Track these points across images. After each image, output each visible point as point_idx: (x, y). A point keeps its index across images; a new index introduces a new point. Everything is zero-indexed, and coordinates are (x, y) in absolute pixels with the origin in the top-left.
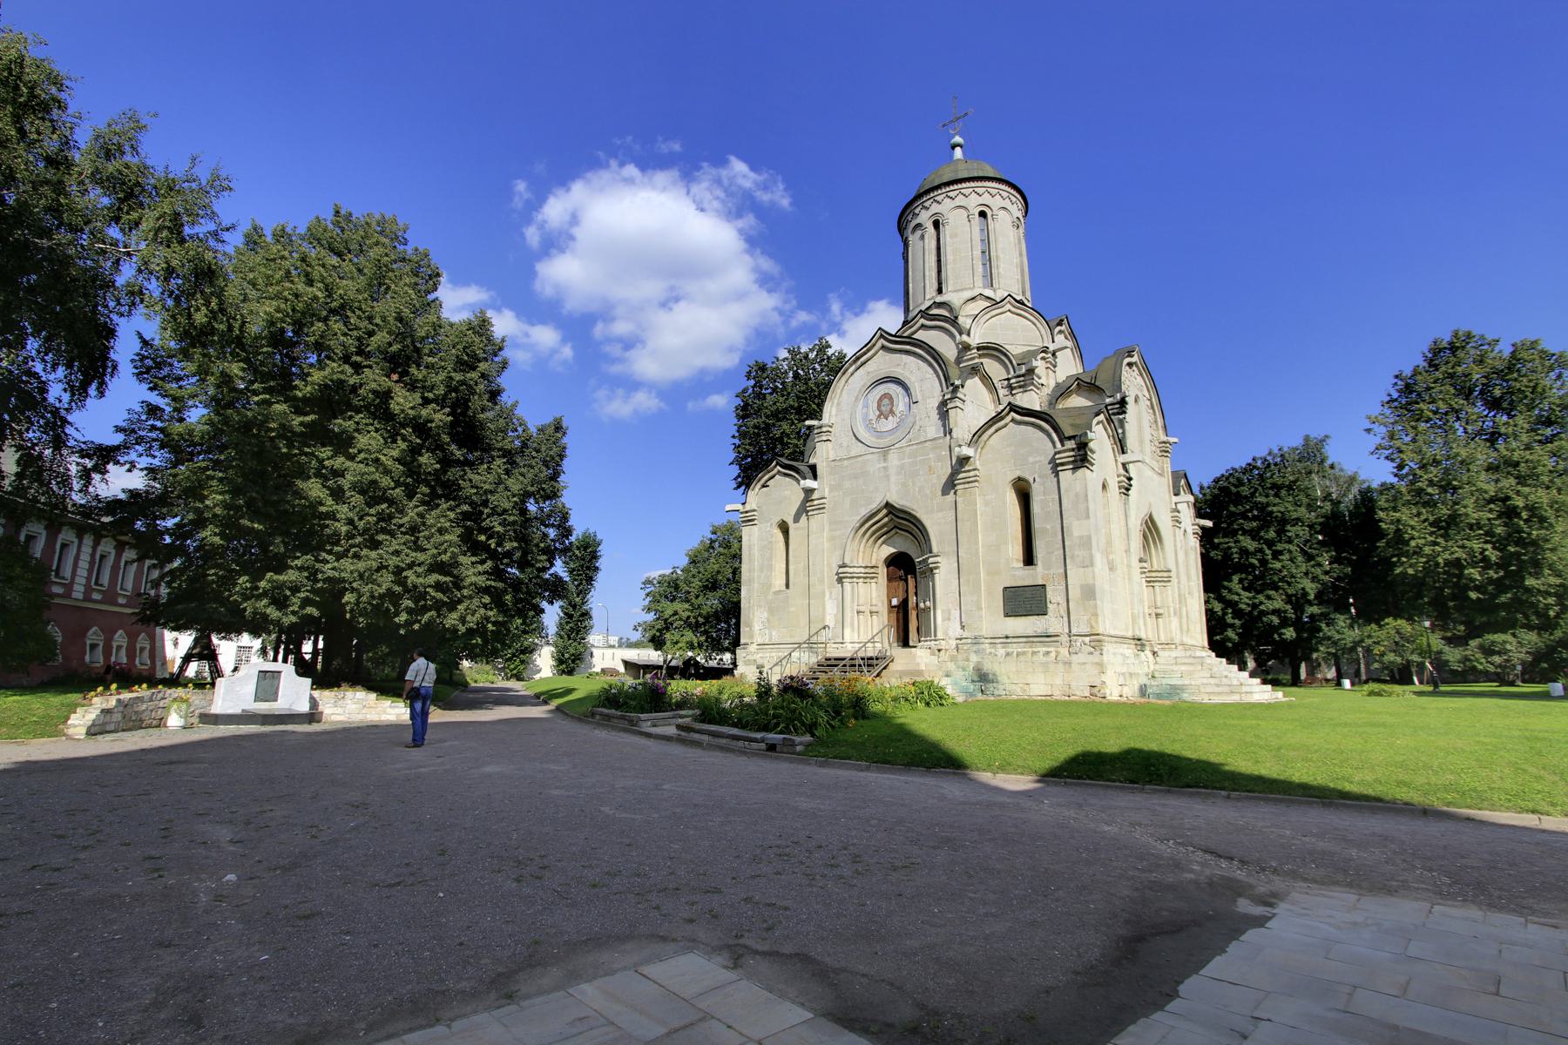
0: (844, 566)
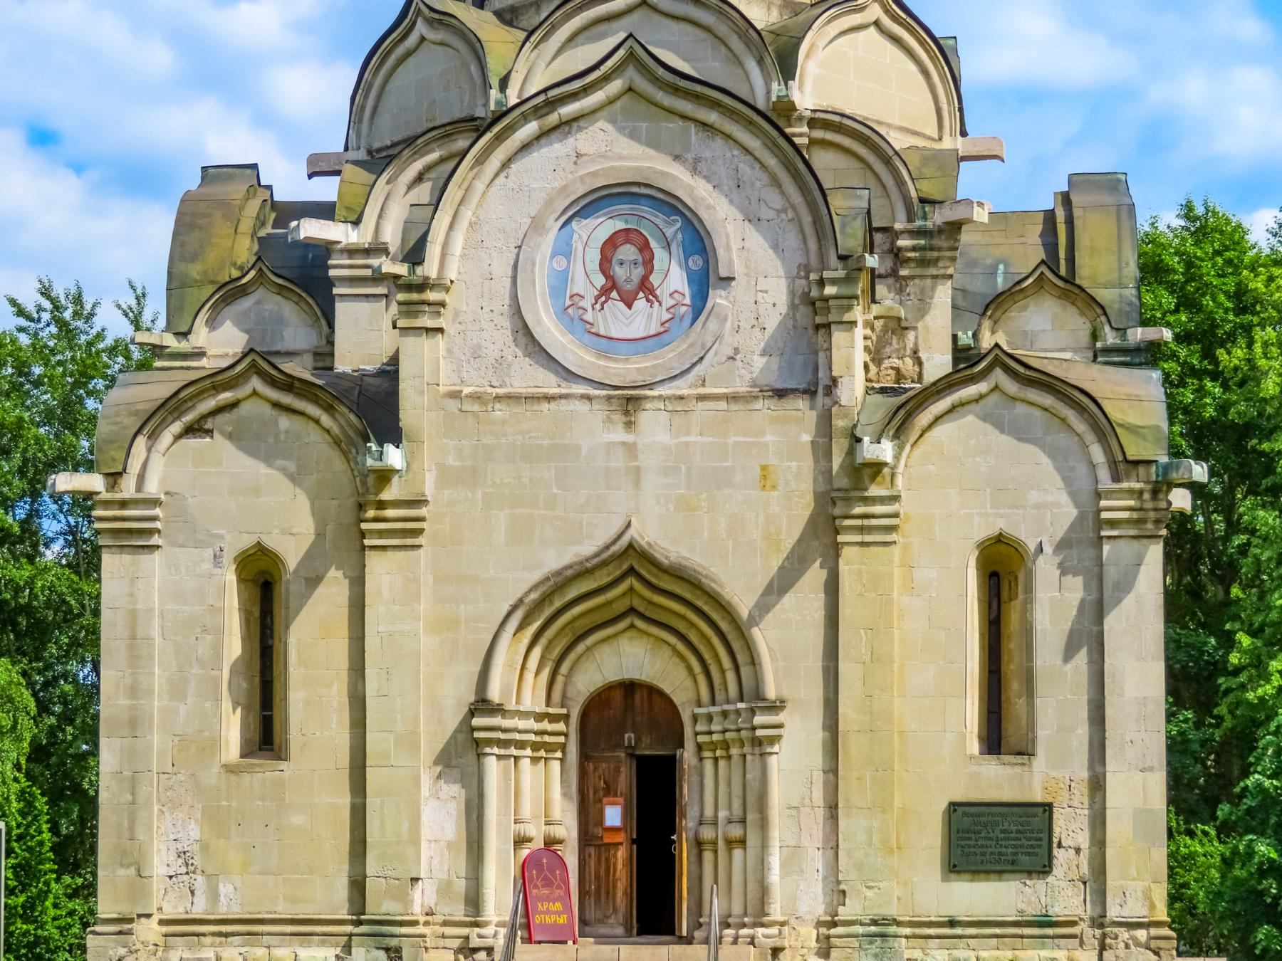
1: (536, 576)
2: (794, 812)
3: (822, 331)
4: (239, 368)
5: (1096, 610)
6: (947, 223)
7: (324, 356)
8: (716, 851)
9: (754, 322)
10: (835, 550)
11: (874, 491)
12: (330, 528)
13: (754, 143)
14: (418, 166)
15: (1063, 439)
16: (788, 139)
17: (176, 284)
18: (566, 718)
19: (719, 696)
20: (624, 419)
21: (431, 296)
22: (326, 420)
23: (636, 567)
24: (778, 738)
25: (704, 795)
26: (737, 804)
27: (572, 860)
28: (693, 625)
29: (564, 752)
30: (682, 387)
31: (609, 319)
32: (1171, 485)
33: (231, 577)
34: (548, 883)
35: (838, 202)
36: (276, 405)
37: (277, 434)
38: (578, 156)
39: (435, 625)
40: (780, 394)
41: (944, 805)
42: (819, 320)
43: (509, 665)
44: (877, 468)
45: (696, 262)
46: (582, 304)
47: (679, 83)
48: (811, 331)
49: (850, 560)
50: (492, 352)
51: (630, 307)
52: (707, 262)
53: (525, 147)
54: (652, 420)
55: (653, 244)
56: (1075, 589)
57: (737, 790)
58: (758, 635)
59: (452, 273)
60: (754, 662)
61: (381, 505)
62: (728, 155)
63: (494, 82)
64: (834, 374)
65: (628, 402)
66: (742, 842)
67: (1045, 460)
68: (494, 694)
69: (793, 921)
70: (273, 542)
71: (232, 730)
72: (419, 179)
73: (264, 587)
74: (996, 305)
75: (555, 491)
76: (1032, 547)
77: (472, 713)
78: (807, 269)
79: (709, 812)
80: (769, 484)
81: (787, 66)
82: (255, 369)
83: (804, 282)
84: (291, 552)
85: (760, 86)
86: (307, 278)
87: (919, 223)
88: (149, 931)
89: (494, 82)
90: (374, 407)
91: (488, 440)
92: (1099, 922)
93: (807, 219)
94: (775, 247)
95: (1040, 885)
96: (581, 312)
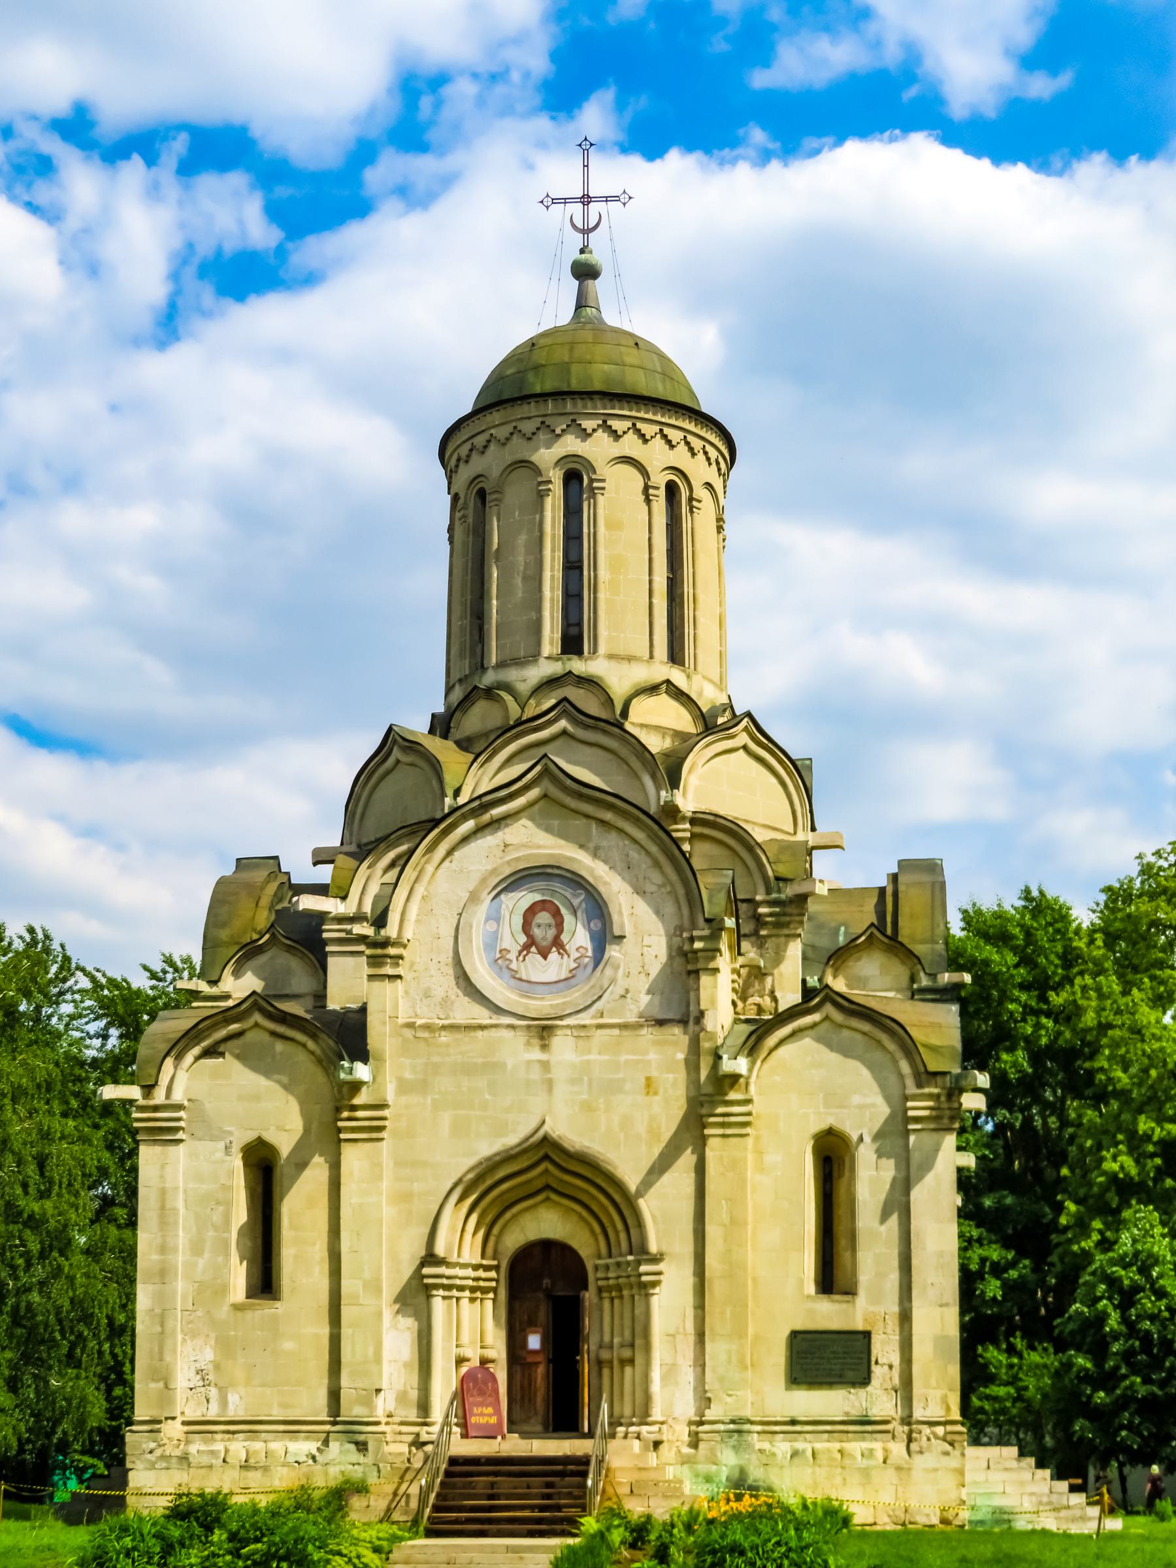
1: (472, 1161)
2: (670, 1338)
3: (693, 976)
5: (904, 1185)
7: (320, 997)
8: (612, 1368)
9: (640, 969)
10: (701, 1144)
11: (733, 1096)
13: (640, 835)
14: (391, 855)
15: (878, 1055)
16: (668, 834)
17: (210, 944)
18: (497, 1268)
20: (540, 1042)
21: (392, 951)
23: (550, 1154)
24: (655, 1284)
25: (600, 1325)
26: (627, 1333)
27: (502, 1376)
28: (593, 1197)
29: (495, 1294)
30: (585, 1019)
32: (961, 1091)
33: (238, 1163)
34: (482, 1393)
35: (706, 882)
38: (506, 846)
39: (396, 1196)
40: (661, 1023)
42: (690, 967)
43: (452, 1228)
44: (734, 1079)
45: (596, 925)
46: (508, 956)
47: (583, 791)
48: (684, 976)
49: (715, 1149)
50: (439, 993)
51: (545, 958)
52: (604, 925)
53: (465, 839)
54: (563, 1045)
55: (563, 911)
56: (888, 1170)
57: (627, 1322)
58: (642, 1203)
59: (408, 934)
60: (640, 1224)
61: (354, 1108)
62: (621, 844)
63: (450, 792)
64: (702, 1007)
65: (543, 1031)
66: (631, 1361)
67: (865, 1073)
68: (440, 1250)
69: (670, 1421)
70: (271, 1137)
71: (238, 1276)
72: (392, 865)
73: (265, 1172)
74: (838, 957)
75: (487, 1097)
76: (855, 1138)
77: (423, 1264)
78: (680, 929)
79: (607, 1338)
80: (651, 1090)
81: (674, 781)
82: (256, 1007)
83: (678, 939)
84: (284, 1145)
85: (655, 796)
86: (307, 940)
87: (774, 895)
88: (173, 1430)
89: (450, 792)
90: (349, 1035)
91: (436, 1059)
92: (907, 1420)
93: (681, 891)
94: (657, 912)
95: (861, 1392)
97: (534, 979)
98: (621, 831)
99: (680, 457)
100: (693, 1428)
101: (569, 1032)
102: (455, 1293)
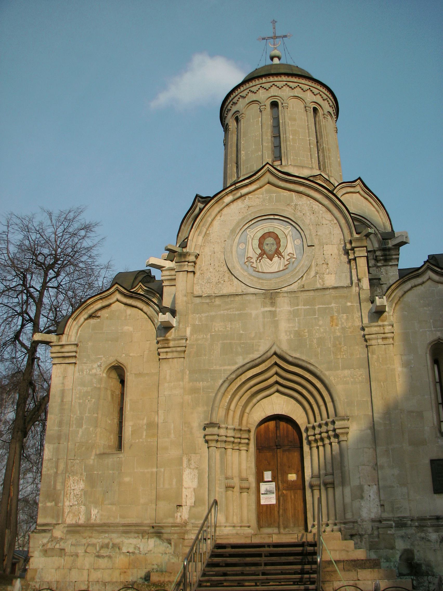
0: (212, 425)
1: (234, 368)
4: (111, 290)
6: (393, 246)
8: (320, 490)
9: (324, 262)
12: (146, 352)
19: (318, 418)
20: (270, 301)
22: (145, 308)
31: (263, 265)
36: (126, 304)
37: (126, 316)
38: (249, 207)
41: (427, 461)
42: (351, 257)
46: (251, 260)
50: (214, 280)
51: (271, 260)
53: (227, 205)
62: (309, 202)
65: (271, 296)
75: (241, 332)
80: (334, 324)
96: (251, 263)
97: (265, 271)
98: (308, 196)
99: (318, 99)
100: (377, 524)
101: (285, 295)
102: (223, 445)
